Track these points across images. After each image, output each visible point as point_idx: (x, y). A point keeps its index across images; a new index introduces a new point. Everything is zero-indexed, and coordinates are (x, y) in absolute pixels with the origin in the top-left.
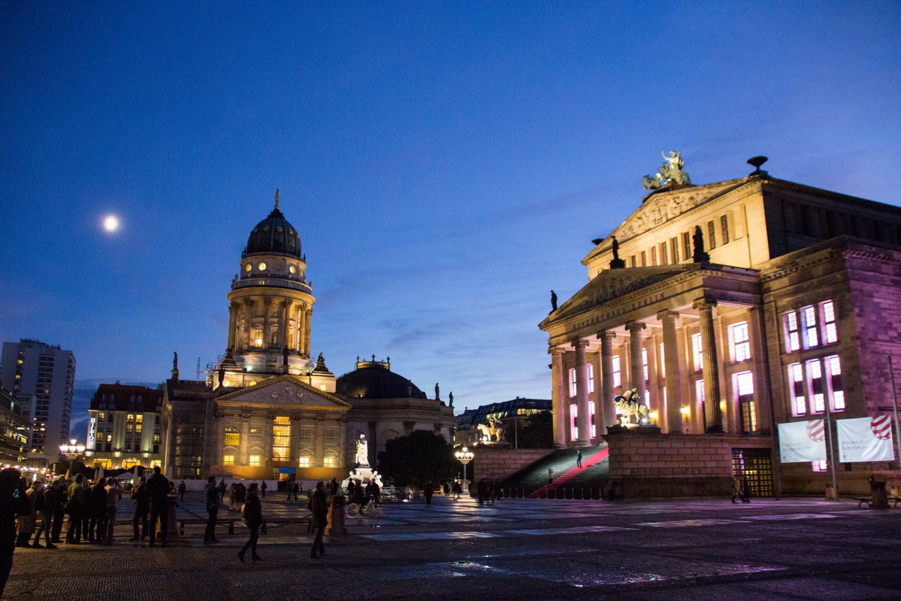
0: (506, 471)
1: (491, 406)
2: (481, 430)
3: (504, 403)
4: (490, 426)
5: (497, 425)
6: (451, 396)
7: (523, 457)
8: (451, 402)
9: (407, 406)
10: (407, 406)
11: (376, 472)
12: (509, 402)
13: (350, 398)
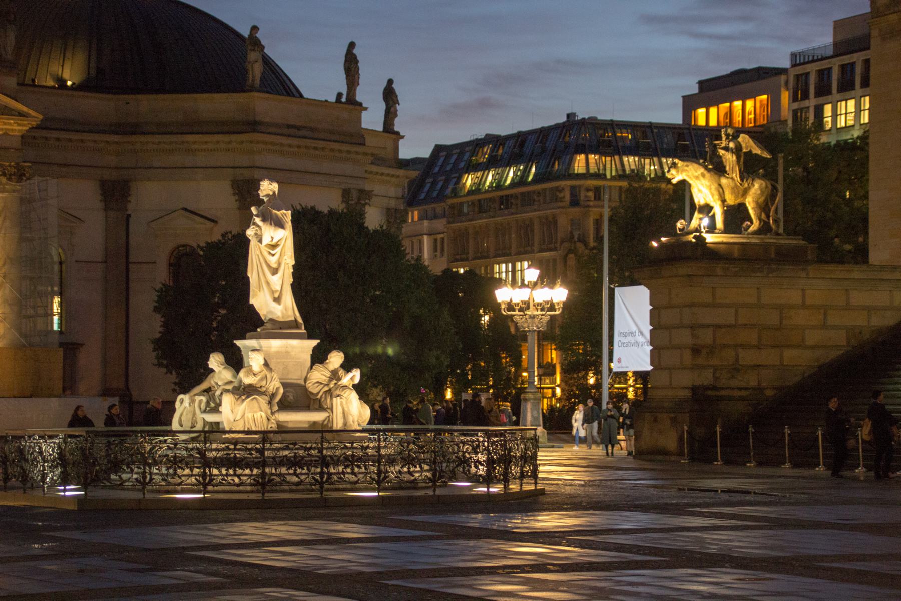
0: (789, 355)
1: (477, 144)
2: (684, 185)
3: (520, 134)
4: (719, 169)
5: (750, 167)
6: (390, 95)
7: (859, 298)
8: (390, 115)
9: (252, 125)
10: (252, 125)
11: (336, 359)
12: (543, 133)
13: (27, 88)
